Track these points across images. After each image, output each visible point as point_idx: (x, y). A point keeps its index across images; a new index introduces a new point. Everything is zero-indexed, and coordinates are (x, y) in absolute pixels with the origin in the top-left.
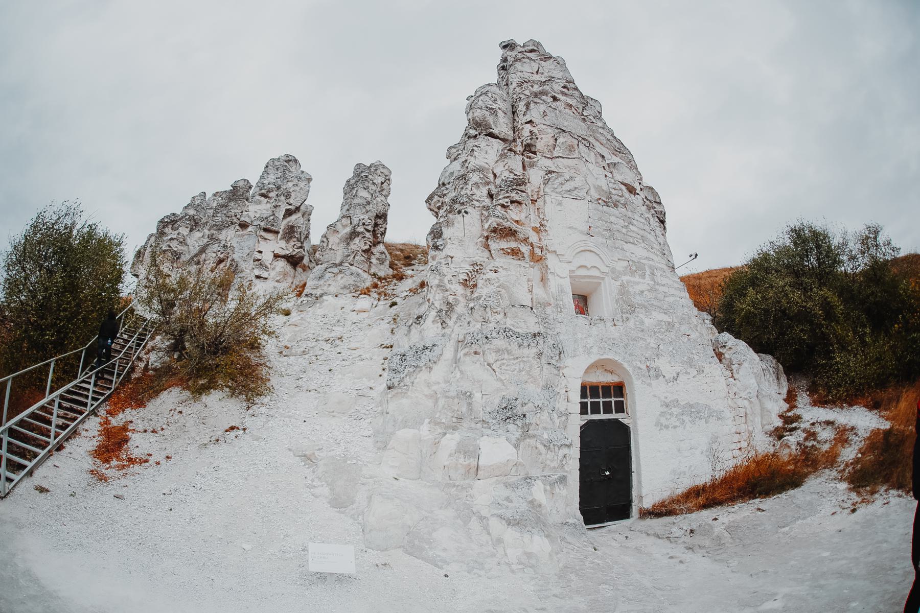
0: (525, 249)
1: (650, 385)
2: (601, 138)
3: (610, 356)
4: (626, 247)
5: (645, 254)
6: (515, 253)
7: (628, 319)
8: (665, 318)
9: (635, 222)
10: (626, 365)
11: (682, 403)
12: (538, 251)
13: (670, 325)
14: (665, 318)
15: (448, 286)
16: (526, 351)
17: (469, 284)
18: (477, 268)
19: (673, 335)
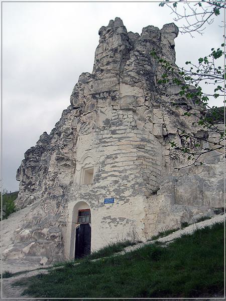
0: (68, 163)
1: (98, 210)
2: (128, 79)
3: (82, 200)
4: (105, 149)
5: (116, 148)
6: (66, 165)
7: (95, 183)
8: (114, 179)
9: (117, 132)
10: (88, 203)
11: (112, 218)
12: (74, 162)
13: (116, 182)
14: (114, 179)
15: (48, 183)
16: (54, 202)
17: (53, 180)
18: (56, 174)
19: (116, 187)
